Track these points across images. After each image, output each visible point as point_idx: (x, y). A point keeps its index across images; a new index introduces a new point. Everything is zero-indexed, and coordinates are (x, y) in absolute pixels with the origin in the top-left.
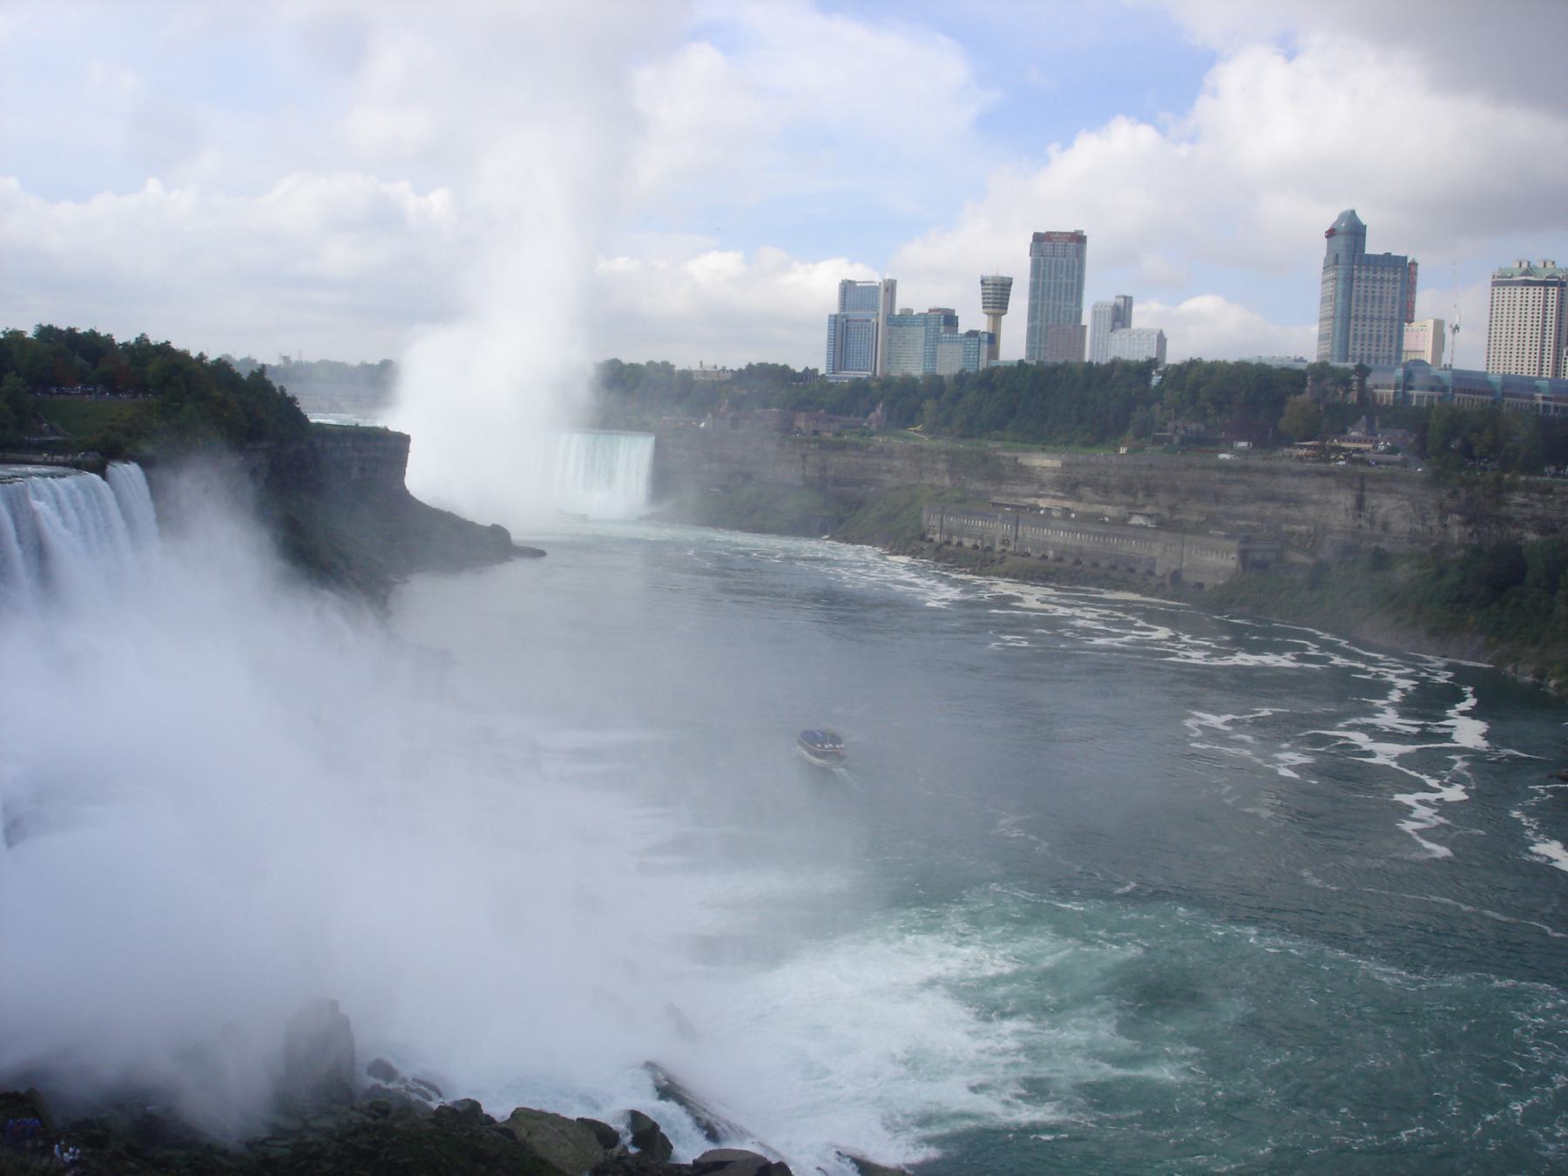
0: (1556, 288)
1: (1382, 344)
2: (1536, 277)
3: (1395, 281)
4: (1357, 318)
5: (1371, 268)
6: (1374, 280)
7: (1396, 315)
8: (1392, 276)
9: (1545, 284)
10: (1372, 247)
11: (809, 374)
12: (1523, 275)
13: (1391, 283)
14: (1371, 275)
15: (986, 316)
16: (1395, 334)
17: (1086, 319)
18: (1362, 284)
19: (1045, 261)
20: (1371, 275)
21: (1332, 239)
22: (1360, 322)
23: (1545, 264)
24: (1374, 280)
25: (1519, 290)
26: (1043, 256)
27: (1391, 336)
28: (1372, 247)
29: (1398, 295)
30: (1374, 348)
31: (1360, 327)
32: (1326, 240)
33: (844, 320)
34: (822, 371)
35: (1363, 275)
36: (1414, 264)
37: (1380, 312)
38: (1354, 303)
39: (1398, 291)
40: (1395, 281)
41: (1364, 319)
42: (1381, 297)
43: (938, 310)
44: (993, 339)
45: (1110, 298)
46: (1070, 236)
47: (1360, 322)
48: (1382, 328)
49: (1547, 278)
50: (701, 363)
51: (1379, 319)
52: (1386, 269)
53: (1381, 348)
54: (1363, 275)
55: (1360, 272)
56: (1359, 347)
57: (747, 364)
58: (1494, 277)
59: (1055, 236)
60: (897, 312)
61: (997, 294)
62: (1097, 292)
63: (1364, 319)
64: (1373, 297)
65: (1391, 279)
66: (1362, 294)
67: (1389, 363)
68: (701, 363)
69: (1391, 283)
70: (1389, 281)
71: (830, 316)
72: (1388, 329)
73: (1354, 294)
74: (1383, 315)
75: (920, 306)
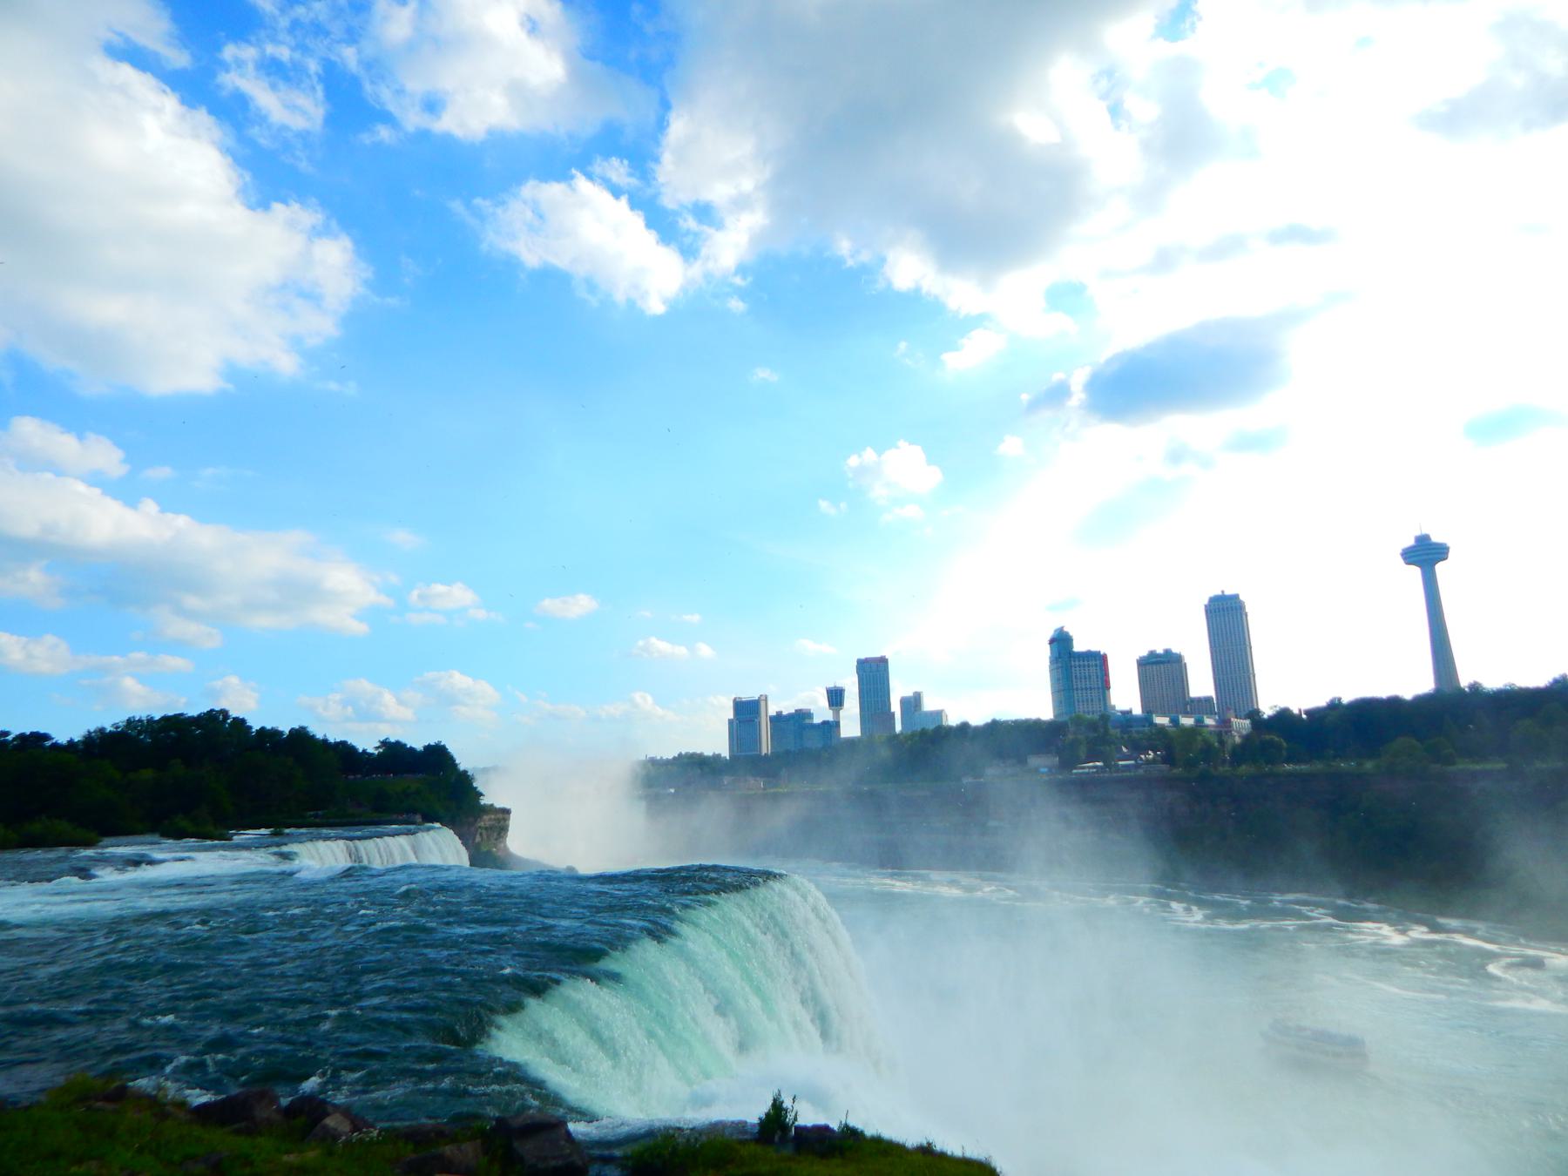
3: (1096, 665)
7: (1100, 686)
10: (1079, 646)
11: (717, 757)
14: (1081, 663)
15: (831, 711)
16: (1101, 698)
17: (896, 707)
20: (1081, 663)
21: (1055, 643)
22: (1080, 692)
25: (1154, 667)
28: (1079, 646)
29: (1099, 671)
30: (1090, 707)
32: (1048, 646)
34: (725, 753)
35: (1077, 663)
38: (1074, 680)
41: (1082, 689)
42: (1090, 676)
43: (800, 710)
44: (837, 724)
45: (909, 693)
47: (1080, 692)
51: (1091, 689)
54: (1077, 663)
55: (1074, 661)
56: (1081, 707)
57: (678, 752)
58: (1137, 661)
60: (772, 711)
61: (836, 697)
62: (898, 691)
63: (1082, 689)
71: (729, 720)
73: (1074, 675)
74: (1092, 686)
75: (788, 708)
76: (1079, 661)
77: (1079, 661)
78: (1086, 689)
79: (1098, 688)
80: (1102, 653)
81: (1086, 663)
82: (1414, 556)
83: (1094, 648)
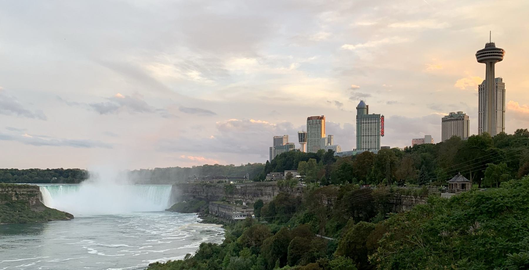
0: (461, 121)
1: (372, 144)
2: (454, 118)
3: (375, 123)
4: (375, 136)
5: (365, 119)
6: (368, 123)
8: (374, 121)
9: (457, 120)
12: (450, 117)
13: (374, 124)
14: (367, 121)
15: (300, 144)
18: (365, 124)
19: (310, 126)
20: (367, 121)
23: (459, 114)
24: (368, 123)
26: (310, 124)
27: (375, 141)
31: (365, 139)
33: (274, 149)
35: (365, 122)
36: (383, 117)
37: (371, 133)
39: (377, 126)
40: (375, 123)
41: (366, 136)
46: (317, 117)
48: (372, 139)
49: (458, 117)
50: (242, 164)
51: (371, 136)
52: (372, 119)
53: (372, 145)
54: (365, 122)
55: (363, 121)
59: (313, 118)
64: (368, 128)
65: (374, 122)
66: (365, 128)
67: (373, 150)
68: (242, 164)
69: (374, 124)
70: (373, 123)
72: (374, 139)
76: (366, 120)
77: (366, 120)
78: (368, 136)
79: (375, 136)
80: (381, 115)
81: (370, 121)
82: (481, 57)
83: (376, 113)
